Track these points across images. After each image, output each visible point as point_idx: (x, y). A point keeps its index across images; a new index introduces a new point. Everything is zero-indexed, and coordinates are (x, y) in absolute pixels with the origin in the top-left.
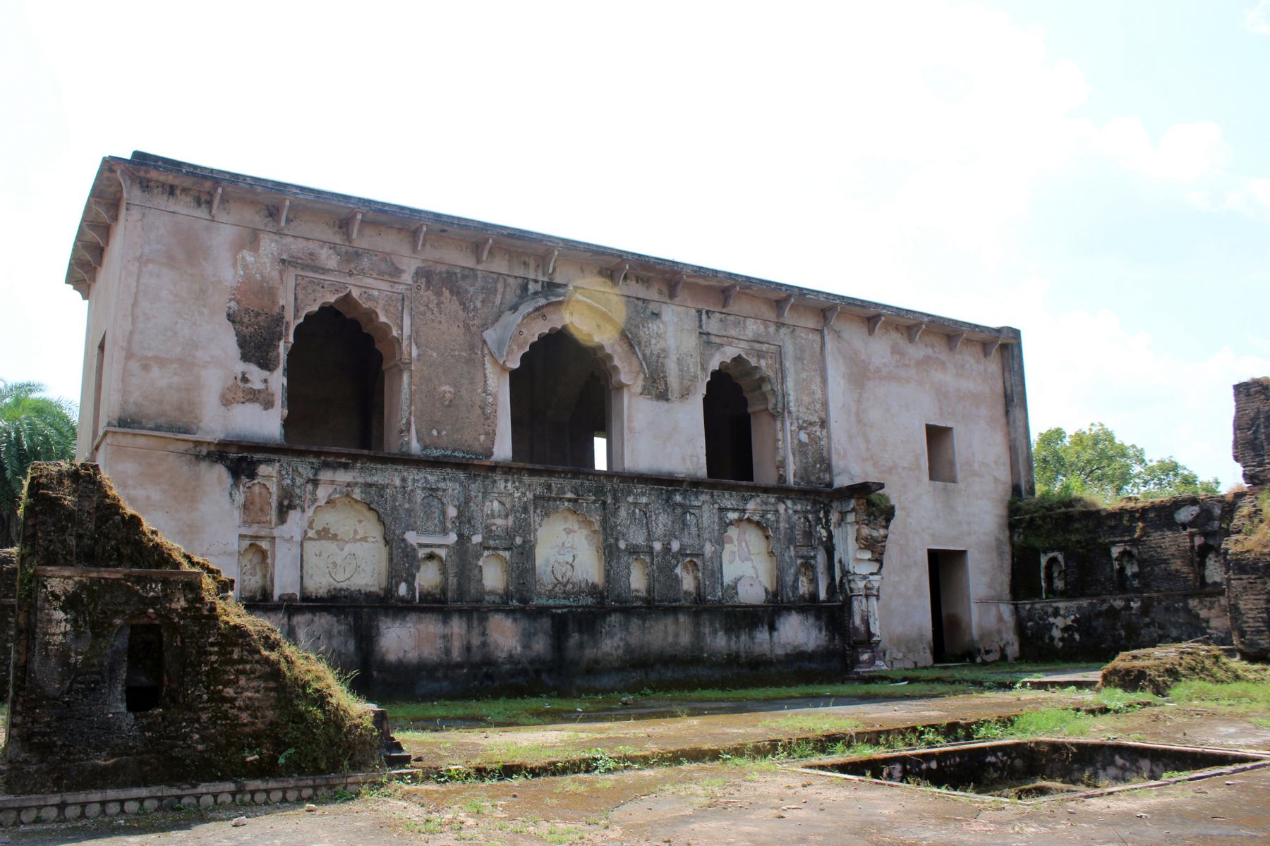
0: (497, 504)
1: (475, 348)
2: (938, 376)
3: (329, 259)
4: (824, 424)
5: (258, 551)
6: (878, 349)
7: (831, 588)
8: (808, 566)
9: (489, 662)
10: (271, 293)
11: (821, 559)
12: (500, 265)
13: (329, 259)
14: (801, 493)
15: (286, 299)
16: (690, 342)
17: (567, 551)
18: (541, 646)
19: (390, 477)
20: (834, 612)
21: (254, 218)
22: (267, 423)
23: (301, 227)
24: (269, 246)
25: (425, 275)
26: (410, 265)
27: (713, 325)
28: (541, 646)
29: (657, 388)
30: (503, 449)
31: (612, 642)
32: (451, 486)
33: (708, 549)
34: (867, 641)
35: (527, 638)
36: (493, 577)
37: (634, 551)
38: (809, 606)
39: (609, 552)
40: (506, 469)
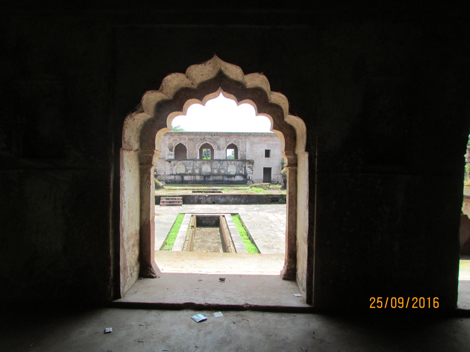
0: (198, 164)
1: (195, 146)
2: (268, 142)
3: (178, 139)
4: (245, 151)
5: (171, 169)
6: (256, 139)
7: (245, 173)
8: (241, 169)
9: (196, 180)
10: (172, 144)
11: (243, 169)
12: (198, 137)
13: (178, 139)
14: (240, 160)
15: (173, 144)
16: (224, 142)
17: (206, 169)
18: (202, 179)
19: (185, 162)
20: (245, 176)
21: (170, 136)
22: (172, 157)
23: (175, 136)
24: (172, 139)
25: (189, 139)
26: (187, 138)
27: (228, 140)
28: (202, 179)
29: (219, 149)
30: (198, 158)
31: (211, 179)
32: (192, 162)
33: (225, 168)
34: (249, 180)
35: (201, 178)
36: (197, 171)
37: (215, 168)
38: (240, 175)
39: (212, 168)
40: (198, 160)
